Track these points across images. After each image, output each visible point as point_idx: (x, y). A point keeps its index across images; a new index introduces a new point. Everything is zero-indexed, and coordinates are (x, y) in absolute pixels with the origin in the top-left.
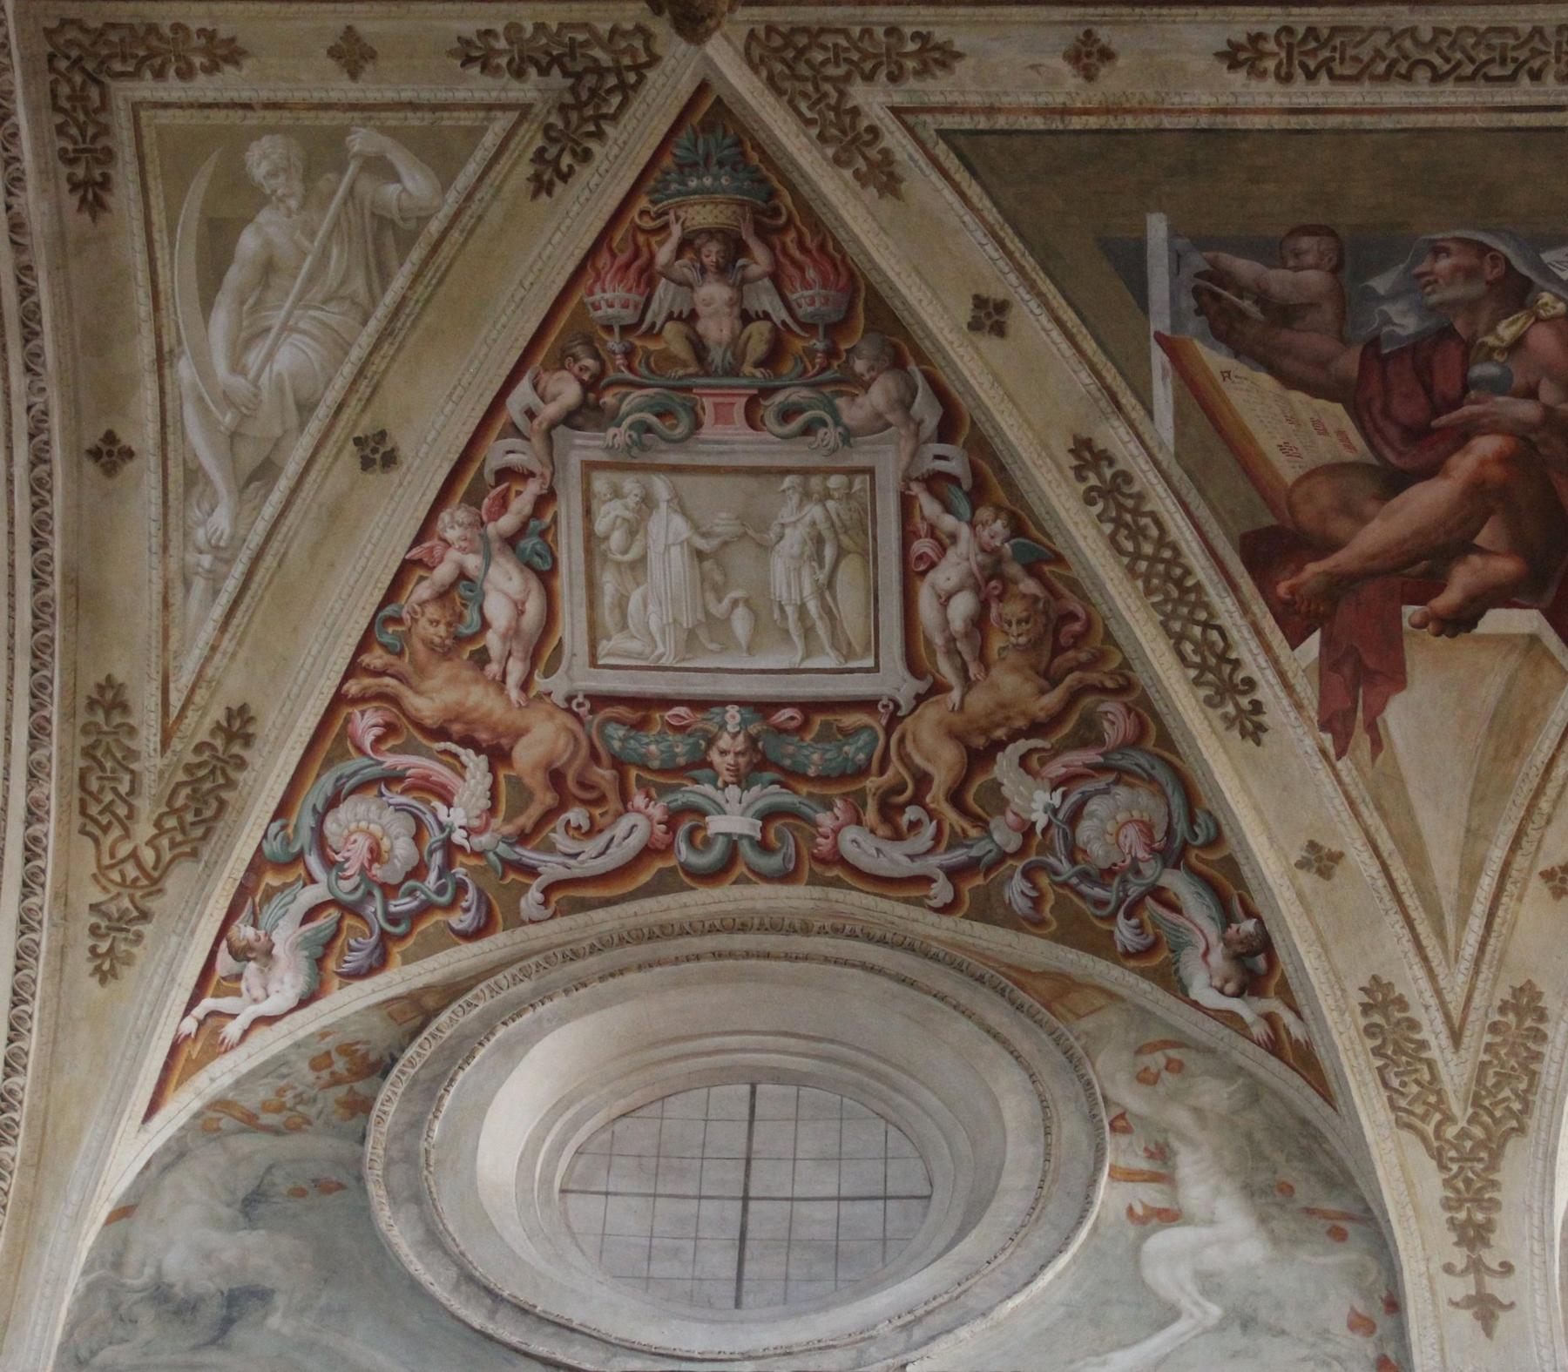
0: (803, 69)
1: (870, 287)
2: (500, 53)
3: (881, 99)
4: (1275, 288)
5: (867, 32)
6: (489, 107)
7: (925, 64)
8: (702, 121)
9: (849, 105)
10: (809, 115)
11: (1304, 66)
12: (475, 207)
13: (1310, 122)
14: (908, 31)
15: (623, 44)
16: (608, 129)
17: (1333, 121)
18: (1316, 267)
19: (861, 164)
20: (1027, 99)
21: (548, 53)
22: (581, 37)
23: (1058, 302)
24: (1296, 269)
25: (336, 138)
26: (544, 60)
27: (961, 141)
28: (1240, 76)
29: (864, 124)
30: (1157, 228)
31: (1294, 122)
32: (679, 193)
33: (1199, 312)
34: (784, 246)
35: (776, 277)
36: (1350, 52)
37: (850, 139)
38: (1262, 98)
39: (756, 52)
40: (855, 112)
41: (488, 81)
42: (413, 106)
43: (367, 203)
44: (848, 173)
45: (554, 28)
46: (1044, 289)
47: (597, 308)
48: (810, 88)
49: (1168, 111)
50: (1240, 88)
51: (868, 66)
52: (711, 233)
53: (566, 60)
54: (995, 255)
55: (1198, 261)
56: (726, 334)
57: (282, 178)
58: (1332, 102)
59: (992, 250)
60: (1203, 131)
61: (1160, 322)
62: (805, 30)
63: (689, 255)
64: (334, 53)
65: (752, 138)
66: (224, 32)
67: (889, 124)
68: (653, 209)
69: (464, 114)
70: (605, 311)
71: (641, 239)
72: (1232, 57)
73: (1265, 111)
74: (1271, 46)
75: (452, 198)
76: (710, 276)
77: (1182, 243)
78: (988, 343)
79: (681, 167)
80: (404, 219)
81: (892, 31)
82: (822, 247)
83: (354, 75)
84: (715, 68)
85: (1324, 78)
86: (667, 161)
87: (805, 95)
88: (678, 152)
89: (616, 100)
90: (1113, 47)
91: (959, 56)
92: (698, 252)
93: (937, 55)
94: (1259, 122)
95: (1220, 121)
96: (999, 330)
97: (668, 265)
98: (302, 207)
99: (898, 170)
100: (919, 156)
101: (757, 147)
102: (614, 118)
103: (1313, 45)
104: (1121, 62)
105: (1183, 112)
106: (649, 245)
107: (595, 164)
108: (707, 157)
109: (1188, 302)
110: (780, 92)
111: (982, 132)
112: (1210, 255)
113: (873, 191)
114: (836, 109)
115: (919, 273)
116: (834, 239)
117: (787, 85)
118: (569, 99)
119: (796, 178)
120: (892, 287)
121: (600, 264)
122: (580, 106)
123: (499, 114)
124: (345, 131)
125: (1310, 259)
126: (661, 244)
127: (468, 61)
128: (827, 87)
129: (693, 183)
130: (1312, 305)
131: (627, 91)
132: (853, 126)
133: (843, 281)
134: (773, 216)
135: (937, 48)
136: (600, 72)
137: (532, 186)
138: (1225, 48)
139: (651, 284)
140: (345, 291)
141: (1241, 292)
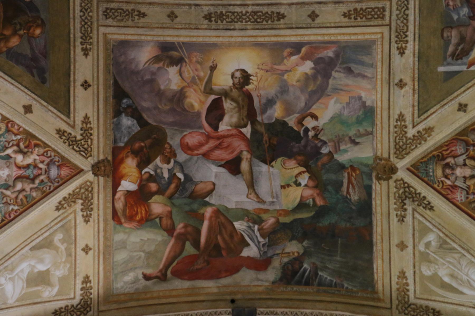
0: (404, 147)
1: (456, 135)
2: (401, 213)
3: (411, 130)
4: (456, 41)
5: (396, 132)
6: (413, 218)
7: (402, 120)
8: (417, 170)
9: (412, 137)
10: (414, 146)
11: (404, 38)
12: (437, 225)
13: (417, 36)
14: (395, 124)
15: (399, 186)
16: (418, 192)
17: (417, 31)
18: (451, 32)
19: (426, 135)
20: (411, 98)
21: (401, 203)
22: (397, 195)
23: (459, 92)
24: (451, 37)
25: (421, 254)
26: (402, 204)
27: (421, 112)
28: (406, 52)
29: (416, 134)
30: (441, 69)
31: (417, 39)
32: (434, 177)
33: (461, 59)
34: (446, 154)
35: (454, 157)
36: (401, 28)
37: (420, 138)
38: (411, 47)
39: (400, 157)
40: (414, 136)
41: (407, 217)
42: (414, 235)
43: (436, 250)
44: (428, 139)
45: (395, 201)
46: (456, 95)
47: (462, 200)
48: (408, 146)
49: (414, 67)
50: (409, 52)
51: (403, 133)
52: (443, 171)
53: (403, 199)
54: (448, 106)
55: (449, 60)
56: (469, 170)
57: (431, 268)
58: (412, 31)
59: (446, 107)
60: (419, 59)
61: (464, 68)
62: (395, 146)
63: (449, 177)
64: (402, 250)
65: (420, 159)
66: (398, 274)
67: (417, 129)
68: (437, 184)
69: (415, 224)
70: (463, 198)
71: (445, 187)
72: (402, 53)
73: (414, 46)
74: (400, 45)
75: (435, 229)
76: (454, 172)
77: (445, 63)
78: (469, 108)
79: (427, 176)
80: (440, 241)
81: (395, 127)
82: (447, 146)
83: (407, 247)
84: (404, 166)
85: (407, 33)
86: (426, 179)
87: (410, 147)
88: (423, 176)
89: (411, 189)
90: (399, 79)
91: (401, 113)
92: (448, 174)
93: (401, 117)
94: (417, 47)
95: (417, 55)
96: (466, 106)
97: (451, 182)
98: (437, 265)
99: (427, 127)
100: (424, 123)
101: (422, 158)
102: (415, 190)
103: (399, 36)
104: (403, 78)
105: (414, 64)
106: (446, 186)
107: (426, 196)
108: (425, 170)
109: (459, 61)
110: (409, 153)
111: (419, 108)
112: (448, 57)
113: (432, 133)
114: (413, 140)
115: (452, 124)
116: (444, 143)
117: (408, 151)
118: (411, 199)
119: (429, 150)
120: (455, 130)
121: (451, 198)
122: (413, 197)
123: (415, 216)
124: (420, 251)
125: (449, 34)
126: (446, 182)
127: (403, 221)
128: (408, 142)
129: (431, 174)
130: (460, 33)
131: (409, 187)
132: (417, 137)
133: (454, 141)
134: (440, 156)
135: (399, 117)
136: (405, 192)
137: (432, 211)
138: (400, 55)
139: (456, 186)
140: (457, 258)
141: (457, 49)
